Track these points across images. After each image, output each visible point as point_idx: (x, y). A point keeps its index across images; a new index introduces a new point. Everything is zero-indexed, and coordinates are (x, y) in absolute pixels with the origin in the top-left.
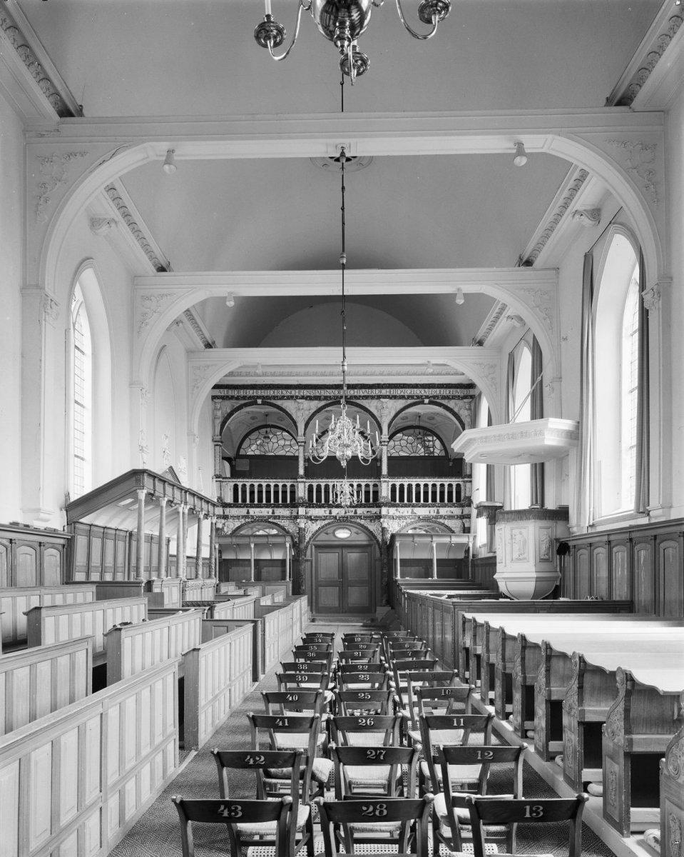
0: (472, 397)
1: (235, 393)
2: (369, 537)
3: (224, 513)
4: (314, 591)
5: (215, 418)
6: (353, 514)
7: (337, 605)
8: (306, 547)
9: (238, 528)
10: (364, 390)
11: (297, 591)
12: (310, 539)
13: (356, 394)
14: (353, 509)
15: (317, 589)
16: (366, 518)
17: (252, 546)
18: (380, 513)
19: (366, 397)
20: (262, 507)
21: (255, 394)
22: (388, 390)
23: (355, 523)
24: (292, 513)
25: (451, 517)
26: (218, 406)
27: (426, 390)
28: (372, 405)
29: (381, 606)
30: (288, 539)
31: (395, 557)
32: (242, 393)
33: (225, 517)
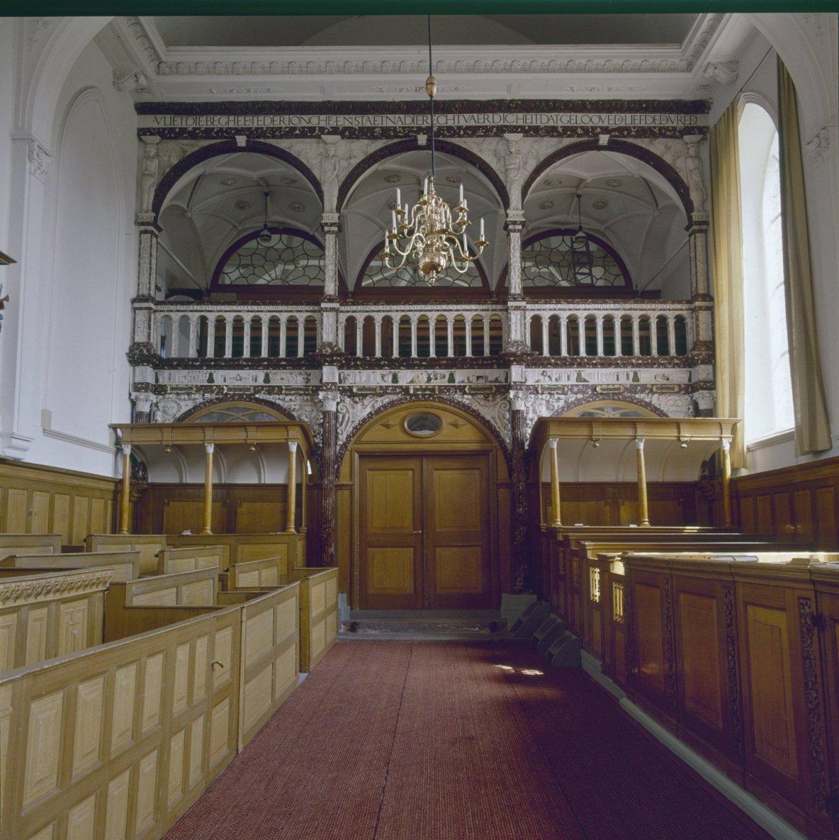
0: (702, 130)
1: (189, 123)
2: (485, 435)
3: (157, 380)
4: (356, 557)
5: (142, 174)
6: (445, 382)
7: (410, 590)
8: (339, 458)
9: (188, 414)
10: (467, 116)
11: (317, 556)
12: (349, 437)
13: (450, 123)
14: (446, 372)
15: (363, 554)
16: (475, 391)
17: (210, 449)
18: (506, 380)
19: (472, 131)
20: (241, 367)
21: (231, 125)
22: (521, 115)
23: (451, 401)
24: (308, 381)
25: (664, 389)
26: (153, 152)
27: (604, 116)
28: (485, 149)
29: (514, 592)
30: (295, 433)
31: (545, 478)
32: (204, 122)
33: (159, 390)
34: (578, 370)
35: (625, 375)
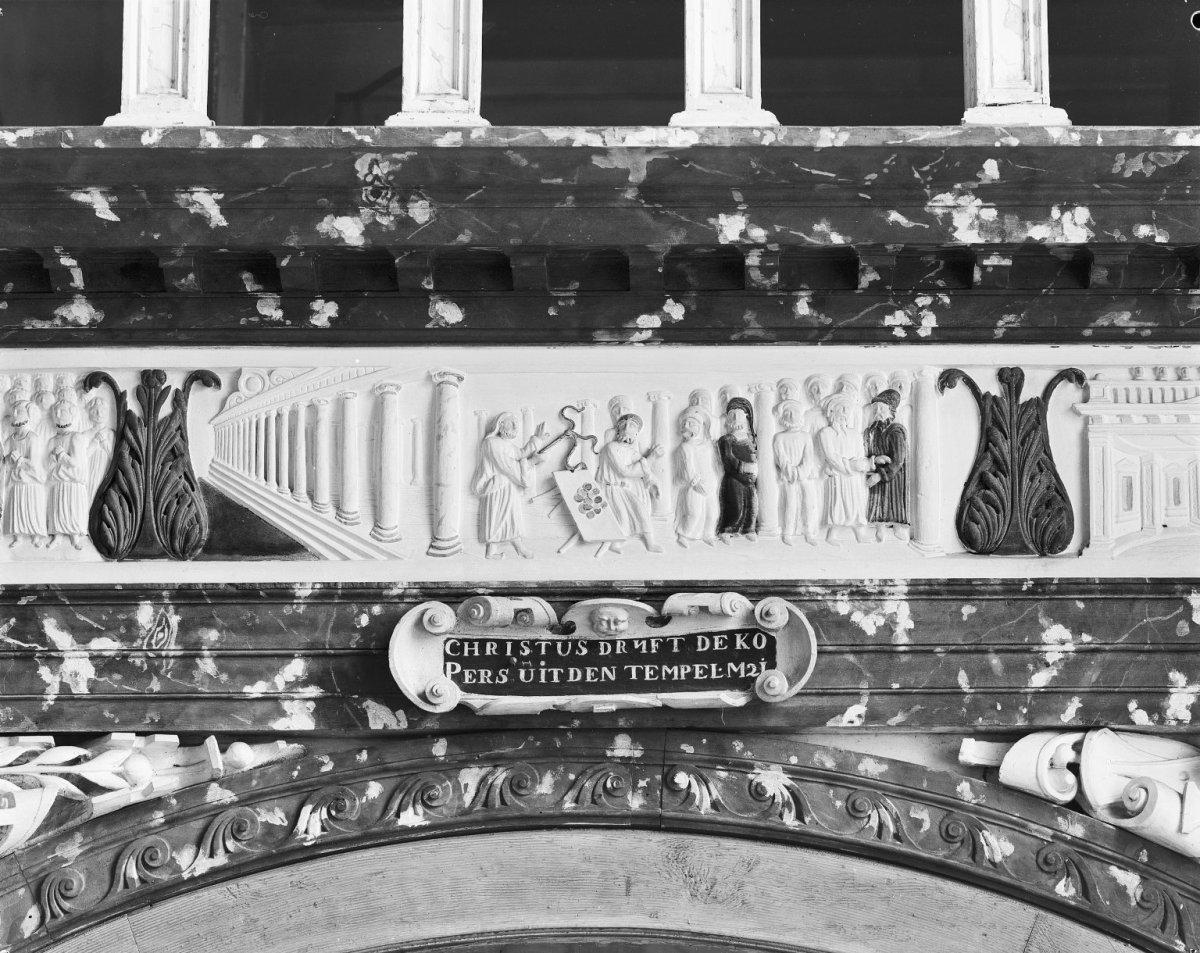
34: (125, 363)
35: (851, 446)
